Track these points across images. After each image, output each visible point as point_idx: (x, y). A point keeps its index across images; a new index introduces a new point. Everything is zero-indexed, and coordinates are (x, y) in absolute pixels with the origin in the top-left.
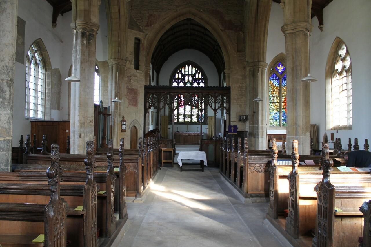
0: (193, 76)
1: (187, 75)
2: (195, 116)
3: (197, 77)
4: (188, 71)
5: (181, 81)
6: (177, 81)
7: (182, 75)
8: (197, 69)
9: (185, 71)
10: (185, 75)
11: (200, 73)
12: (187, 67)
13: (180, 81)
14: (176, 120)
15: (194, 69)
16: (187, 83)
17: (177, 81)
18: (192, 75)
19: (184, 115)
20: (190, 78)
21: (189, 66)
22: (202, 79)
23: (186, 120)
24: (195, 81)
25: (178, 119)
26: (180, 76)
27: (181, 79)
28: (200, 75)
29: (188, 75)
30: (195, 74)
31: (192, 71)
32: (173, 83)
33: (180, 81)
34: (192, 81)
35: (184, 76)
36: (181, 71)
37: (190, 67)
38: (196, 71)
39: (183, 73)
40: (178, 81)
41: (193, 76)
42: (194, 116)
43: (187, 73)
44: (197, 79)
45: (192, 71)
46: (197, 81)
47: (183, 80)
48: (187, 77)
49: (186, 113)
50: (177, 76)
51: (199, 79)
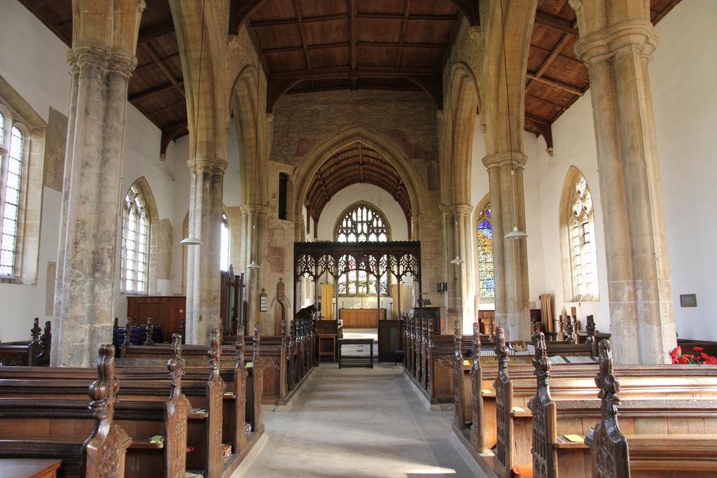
0: (370, 223)
1: (359, 222)
3: (375, 226)
5: (352, 231)
6: (345, 231)
7: (353, 223)
9: (357, 217)
10: (357, 222)
12: (359, 210)
13: (349, 231)
15: (370, 213)
16: (361, 234)
17: (345, 231)
18: (367, 222)
19: (357, 284)
21: (362, 209)
22: (382, 228)
24: (373, 231)
26: (350, 225)
27: (351, 228)
28: (380, 225)
29: (362, 222)
30: (372, 220)
33: (349, 231)
34: (368, 230)
35: (355, 224)
36: (351, 217)
37: (365, 210)
38: (374, 216)
39: (354, 219)
40: (347, 231)
41: (370, 223)
43: (359, 219)
44: (375, 228)
48: (359, 225)
49: (360, 279)
50: (344, 225)
51: (377, 228)
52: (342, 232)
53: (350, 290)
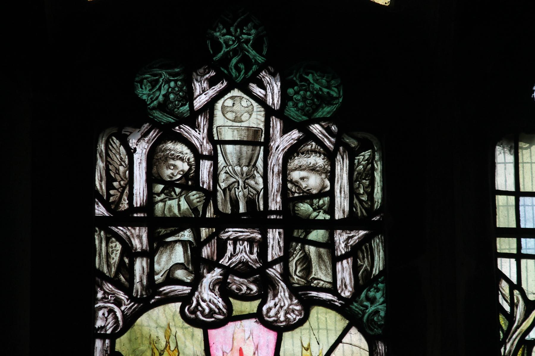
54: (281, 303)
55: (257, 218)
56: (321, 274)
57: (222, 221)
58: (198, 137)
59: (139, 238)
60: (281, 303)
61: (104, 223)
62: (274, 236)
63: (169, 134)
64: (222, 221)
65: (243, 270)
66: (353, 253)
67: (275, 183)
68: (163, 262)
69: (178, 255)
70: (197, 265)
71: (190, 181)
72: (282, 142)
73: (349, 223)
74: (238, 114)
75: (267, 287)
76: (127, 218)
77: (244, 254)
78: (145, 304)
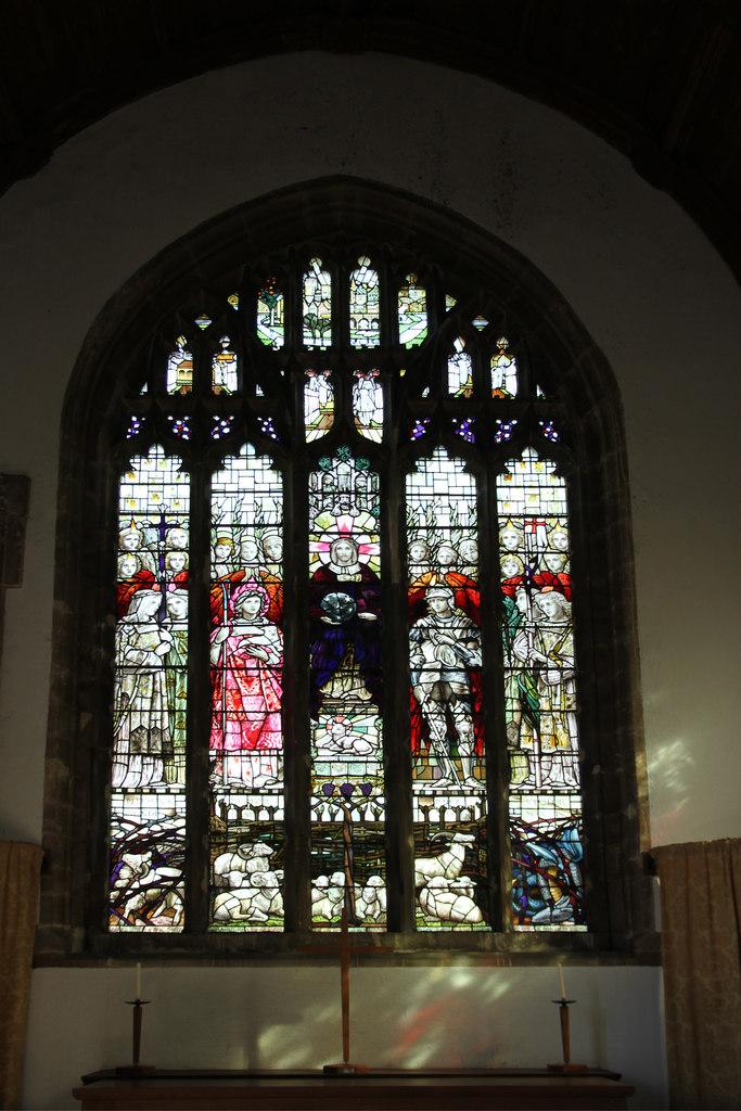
0: (410, 375)
1: (318, 361)
2: (456, 855)
3: (459, 375)
4: (340, 320)
6: (181, 427)
8: (450, 303)
9: (294, 322)
11: (502, 342)
12: (317, 285)
14: (176, 901)
16: (327, 447)
17: (181, 427)
18: (387, 359)
19: (298, 849)
20: (370, 401)
23: (324, 905)
24: (441, 437)
25: (201, 889)
26: (226, 375)
30: (434, 354)
31: (388, 321)
32: (136, 462)
35: (276, 376)
37: (366, 276)
39: (271, 334)
41: (410, 375)
42: (437, 849)
45: (388, 321)
46: (469, 436)
47: (267, 426)
48: (317, 397)
49: (324, 812)
50: (177, 376)
52: (157, 434)
53: (225, 904)
54: (354, 511)
55: (348, 492)
56: (364, 505)
57: (340, 493)
58: (334, 474)
59: (320, 497)
60: (354, 511)
61: (311, 494)
62: (353, 496)
63: (327, 473)
64: (340, 493)
65: (345, 504)
66: (372, 500)
67: (353, 484)
68: (326, 502)
69: (330, 501)
70: (334, 503)
71: (332, 484)
72: (355, 474)
73: (371, 493)
74: (344, 468)
75: (351, 507)
76: (317, 492)
77: (346, 500)
78: (321, 512)
